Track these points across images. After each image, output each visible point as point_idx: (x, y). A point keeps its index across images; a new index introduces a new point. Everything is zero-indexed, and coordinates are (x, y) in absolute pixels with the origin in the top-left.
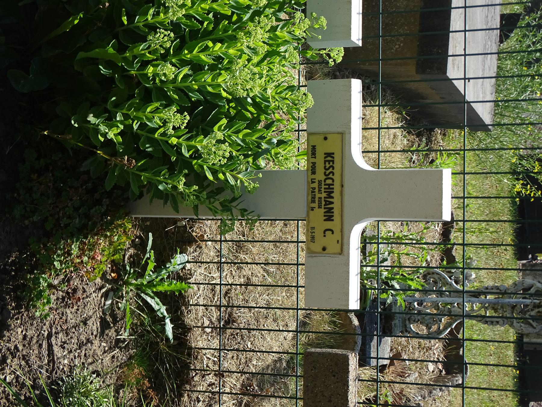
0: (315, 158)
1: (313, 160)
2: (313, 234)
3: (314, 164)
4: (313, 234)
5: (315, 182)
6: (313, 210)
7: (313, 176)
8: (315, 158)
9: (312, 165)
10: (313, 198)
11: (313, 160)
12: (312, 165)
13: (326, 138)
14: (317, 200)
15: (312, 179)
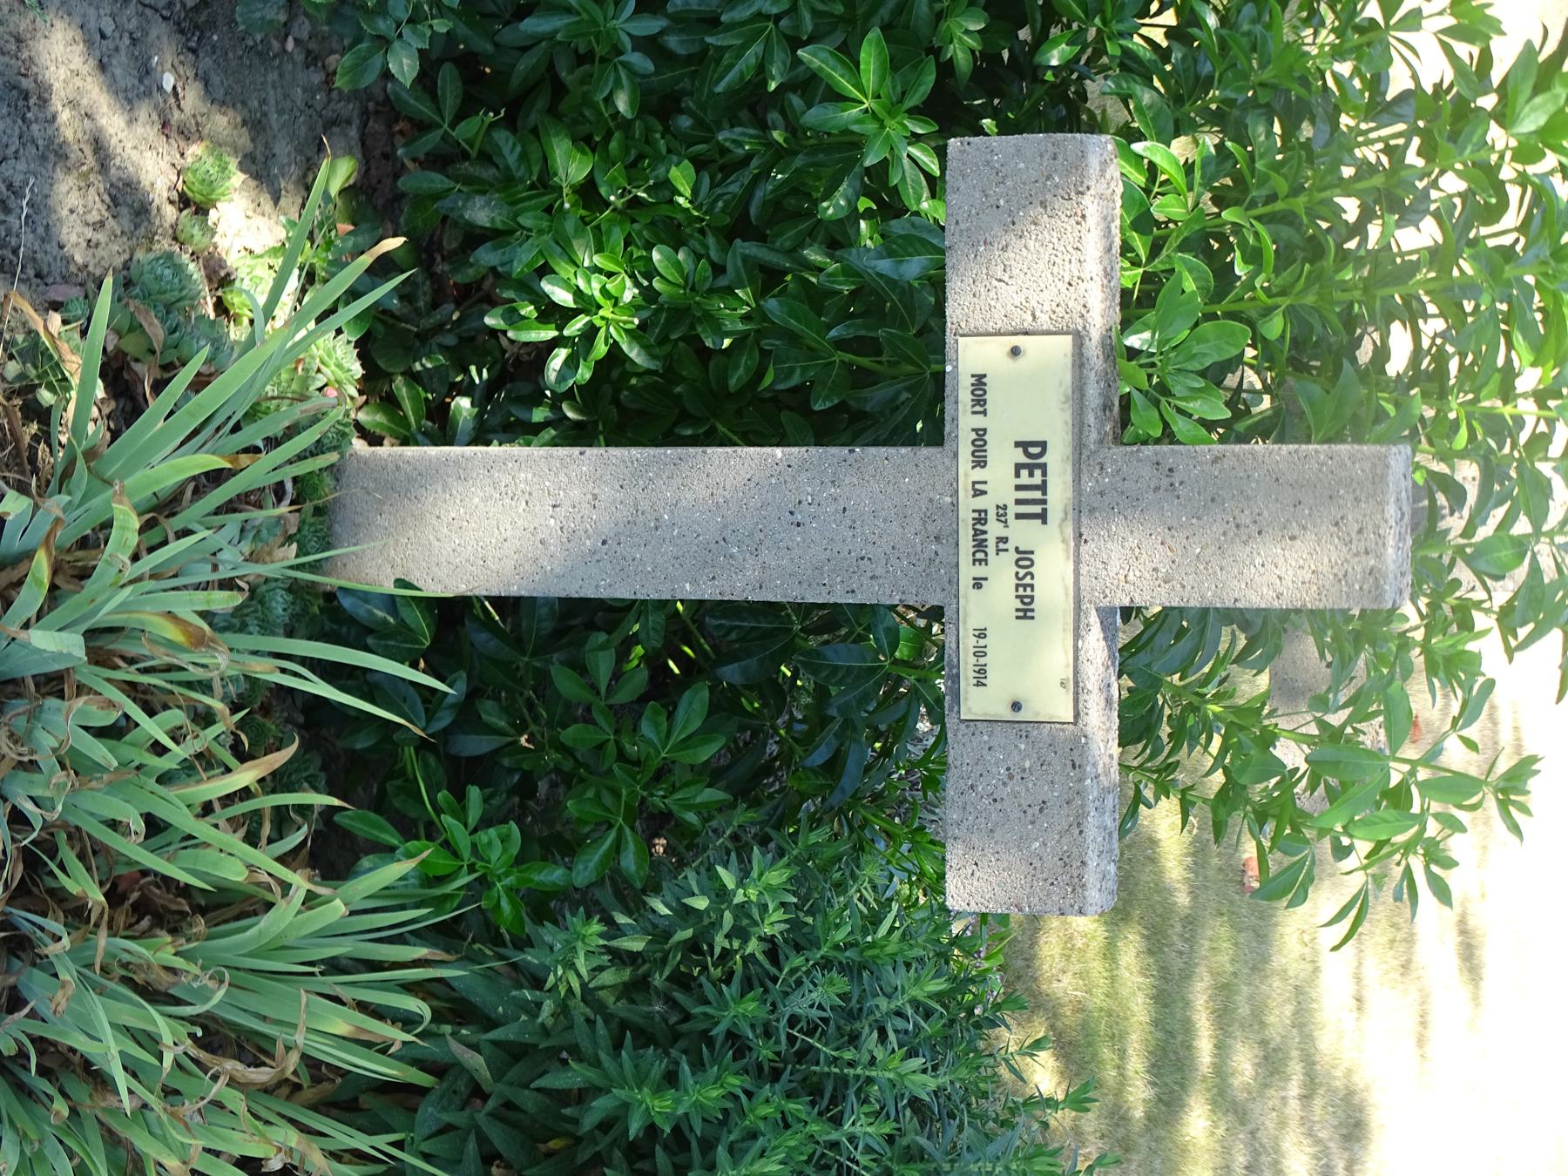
0: (984, 413)
1: (979, 421)
2: (982, 661)
3: (981, 433)
4: (982, 661)
5: (984, 493)
6: (978, 583)
7: (978, 474)
8: (984, 413)
9: (974, 436)
10: (980, 545)
11: (979, 421)
12: (974, 436)
13: (1015, 352)
14: (991, 549)
15: (974, 483)
